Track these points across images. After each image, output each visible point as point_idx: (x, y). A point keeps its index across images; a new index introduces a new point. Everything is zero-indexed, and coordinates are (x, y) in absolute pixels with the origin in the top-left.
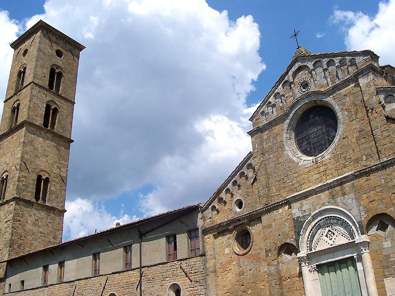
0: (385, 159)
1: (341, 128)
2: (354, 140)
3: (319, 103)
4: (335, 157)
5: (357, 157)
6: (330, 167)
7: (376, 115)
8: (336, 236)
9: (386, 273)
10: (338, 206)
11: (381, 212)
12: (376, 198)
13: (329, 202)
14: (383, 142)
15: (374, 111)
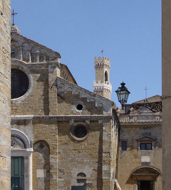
0: (52, 116)
1: (30, 91)
2: (37, 99)
3: (20, 69)
4: (24, 104)
5: (36, 108)
6: (20, 108)
7: (53, 91)
8: (16, 145)
9: (38, 167)
10: (21, 130)
11: (43, 140)
12: (42, 133)
13: (15, 127)
14: (53, 107)
15: (52, 89)
